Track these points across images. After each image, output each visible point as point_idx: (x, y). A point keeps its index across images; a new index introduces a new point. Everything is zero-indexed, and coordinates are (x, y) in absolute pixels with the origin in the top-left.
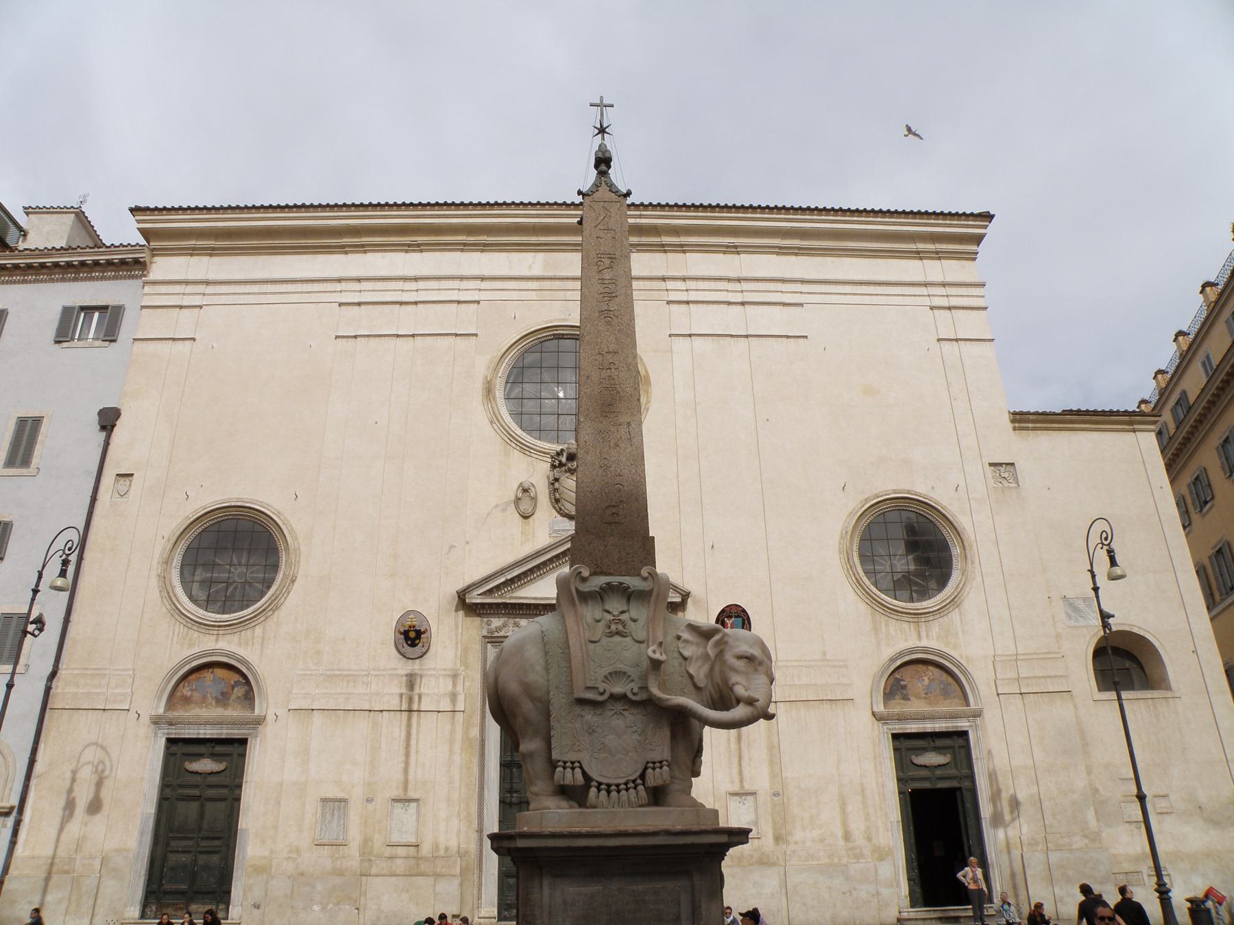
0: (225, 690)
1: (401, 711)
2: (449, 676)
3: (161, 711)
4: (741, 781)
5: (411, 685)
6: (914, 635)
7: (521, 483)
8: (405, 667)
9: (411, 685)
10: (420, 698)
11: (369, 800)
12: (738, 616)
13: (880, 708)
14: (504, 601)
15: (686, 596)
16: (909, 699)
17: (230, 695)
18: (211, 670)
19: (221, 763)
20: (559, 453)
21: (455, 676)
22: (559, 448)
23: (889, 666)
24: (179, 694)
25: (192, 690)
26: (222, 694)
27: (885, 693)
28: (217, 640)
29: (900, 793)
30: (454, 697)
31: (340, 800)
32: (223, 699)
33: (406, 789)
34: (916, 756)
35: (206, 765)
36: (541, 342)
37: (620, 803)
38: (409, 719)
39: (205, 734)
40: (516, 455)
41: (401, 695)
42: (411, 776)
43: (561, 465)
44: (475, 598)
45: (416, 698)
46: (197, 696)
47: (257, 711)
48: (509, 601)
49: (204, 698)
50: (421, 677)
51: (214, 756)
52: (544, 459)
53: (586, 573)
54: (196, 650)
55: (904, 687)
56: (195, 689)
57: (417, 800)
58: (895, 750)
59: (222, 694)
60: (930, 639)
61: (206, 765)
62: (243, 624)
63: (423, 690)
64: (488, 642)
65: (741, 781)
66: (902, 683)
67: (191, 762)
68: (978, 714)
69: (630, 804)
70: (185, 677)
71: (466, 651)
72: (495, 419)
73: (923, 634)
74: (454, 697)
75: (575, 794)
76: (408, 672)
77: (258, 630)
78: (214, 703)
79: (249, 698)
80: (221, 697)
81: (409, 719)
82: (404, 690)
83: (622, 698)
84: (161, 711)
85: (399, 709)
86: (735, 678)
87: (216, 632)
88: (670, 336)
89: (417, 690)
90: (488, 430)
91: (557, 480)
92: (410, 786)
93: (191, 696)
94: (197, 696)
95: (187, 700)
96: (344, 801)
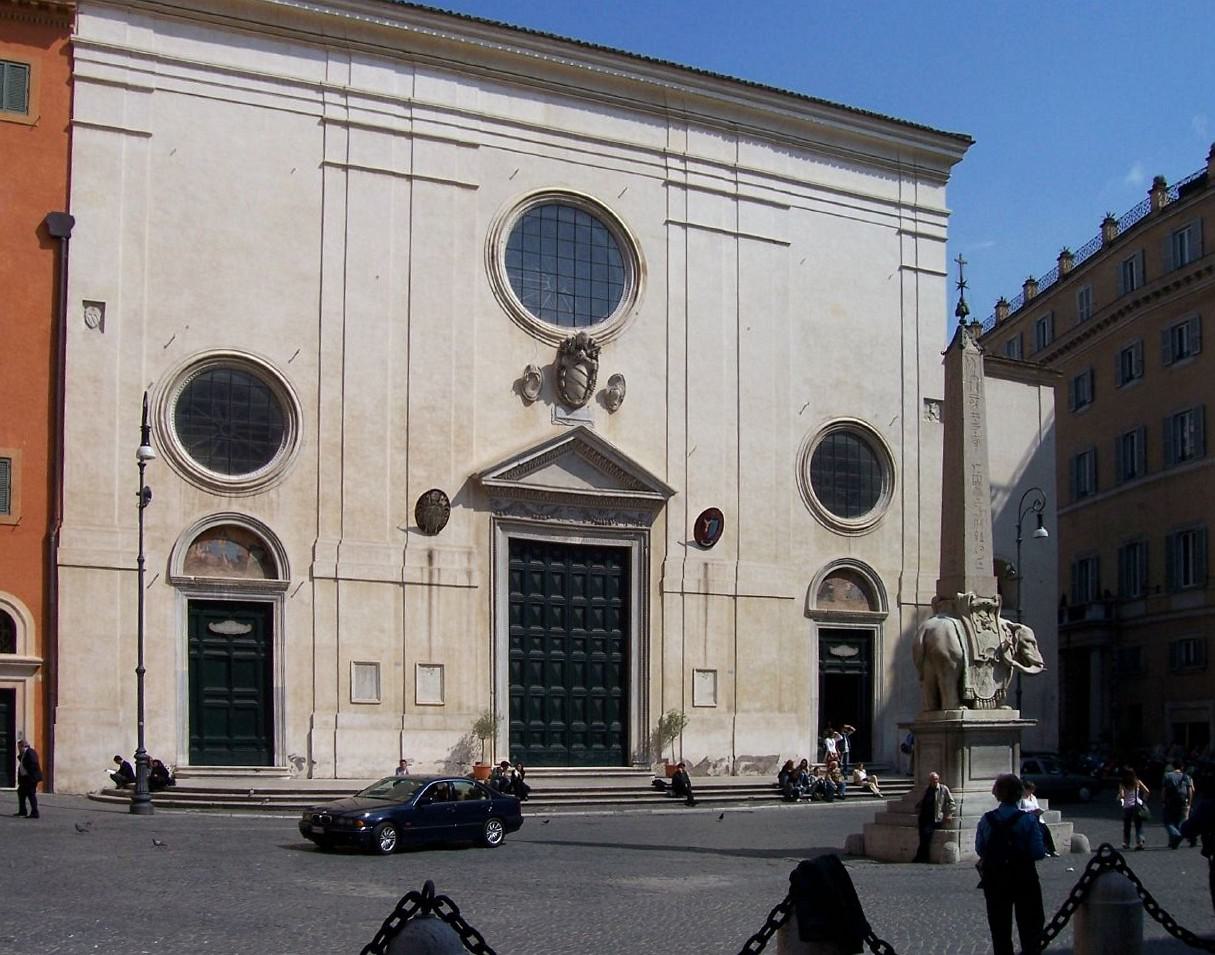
0: (240, 554)
1: (422, 584)
2: (464, 553)
3: (178, 571)
4: (706, 659)
5: (430, 557)
6: (846, 548)
7: (529, 367)
8: (421, 542)
9: (430, 557)
10: (439, 570)
11: (397, 664)
12: (715, 519)
13: (813, 607)
14: (517, 485)
15: (669, 492)
16: (833, 601)
17: (247, 559)
18: (223, 533)
19: (246, 625)
20: (568, 341)
21: (470, 554)
22: (571, 332)
23: (822, 573)
24: (192, 556)
25: (205, 552)
26: (239, 557)
27: (818, 595)
28: (229, 503)
29: (820, 677)
30: (469, 574)
31: (371, 664)
32: (240, 564)
33: (430, 655)
34: (834, 647)
35: (230, 627)
36: (542, 207)
37: (987, 708)
38: (430, 591)
39: (229, 597)
40: (519, 333)
41: (422, 568)
42: (434, 645)
43: (569, 353)
44: (489, 481)
45: (436, 573)
46: (212, 558)
47: (280, 579)
48: (520, 486)
49: (220, 559)
50: (439, 552)
51: (240, 620)
52: (547, 342)
53: (975, 597)
54: (208, 512)
55: (832, 591)
56: (210, 552)
57: (441, 666)
58: (820, 642)
59: (239, 557)
60: (856, 550)
61: (230, 627)
62: (257, 488)
63: (443, 566)
64: (499, 524)
65: (706, 659)
66: (831, 587)
67: (215, 623)
68: (882, 618)
69: (991, 709)
70: (197, 540)
71: (478, 530)
72: (499, 291)
73: (852, 547)
74: (469, 574)
75: (971, 705)
76: (426, 547)
77: (273, 494)
78: (231, 566)
79: (269, 565)
80: (237, 561)
81: (430, 591)
82: (425, 564)
83: (991, 661)
84: (178, 571)
85: (420, 582)
86: (1027, 651)
87: (227, 495)
88: (668, 222)
89: (436, 565)
90: (491, 301)
91: (562, 367)
92: (433, 652)
93: (206, 558)
94: (212, 558)
95: (202, 563)
96: (377, 665)
